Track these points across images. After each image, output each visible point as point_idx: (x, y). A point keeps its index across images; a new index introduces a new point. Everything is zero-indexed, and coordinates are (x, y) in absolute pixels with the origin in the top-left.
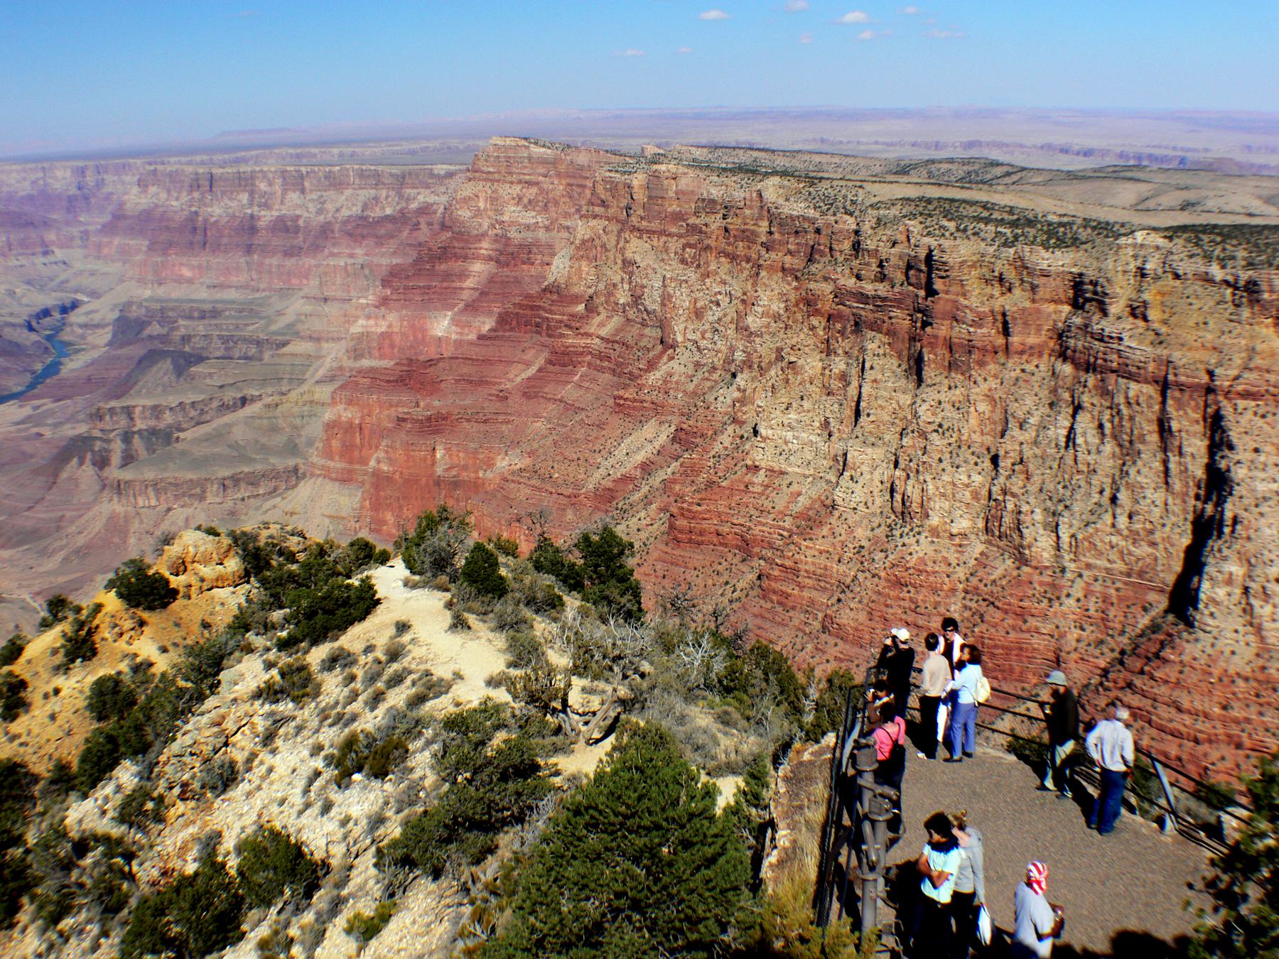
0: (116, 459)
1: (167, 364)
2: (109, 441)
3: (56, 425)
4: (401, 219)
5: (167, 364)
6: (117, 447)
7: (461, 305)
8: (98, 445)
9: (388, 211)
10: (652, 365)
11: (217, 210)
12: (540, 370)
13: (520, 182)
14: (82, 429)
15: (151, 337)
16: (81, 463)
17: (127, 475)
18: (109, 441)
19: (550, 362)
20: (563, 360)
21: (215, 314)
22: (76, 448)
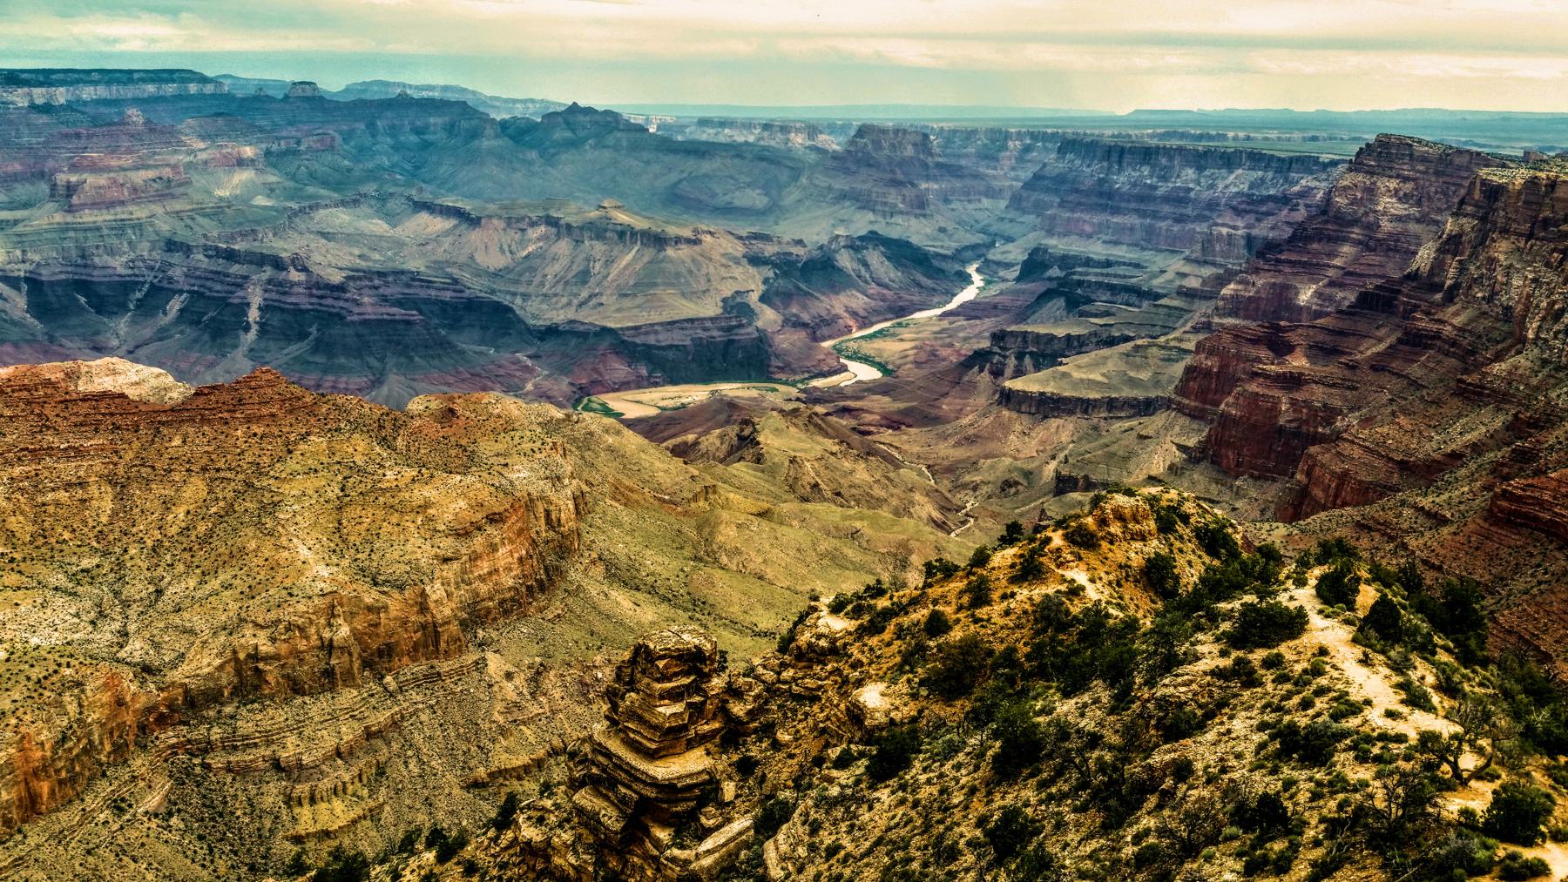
0: (1009, 371)
1: (1061, 302)
2: (1005, 357)
3: (965, 339)
4: (1285, 200)
5: (1061, 302)
6: (1012, 362)
7: (1326, 281)
8: (996, 359)
9: (1272, 192)
10: (1499, 357)
11: (1122, 180)
12: (1390, 347)
13: (1398, 176)
14: (985, 344)
15: (1050, 279)
16: (981, 370)
17: (1017, 385)
18: (1005, 357)
19: (1400, 341)
20: (1415, 342)
21: (1108, 264)
22: (979, 358)
